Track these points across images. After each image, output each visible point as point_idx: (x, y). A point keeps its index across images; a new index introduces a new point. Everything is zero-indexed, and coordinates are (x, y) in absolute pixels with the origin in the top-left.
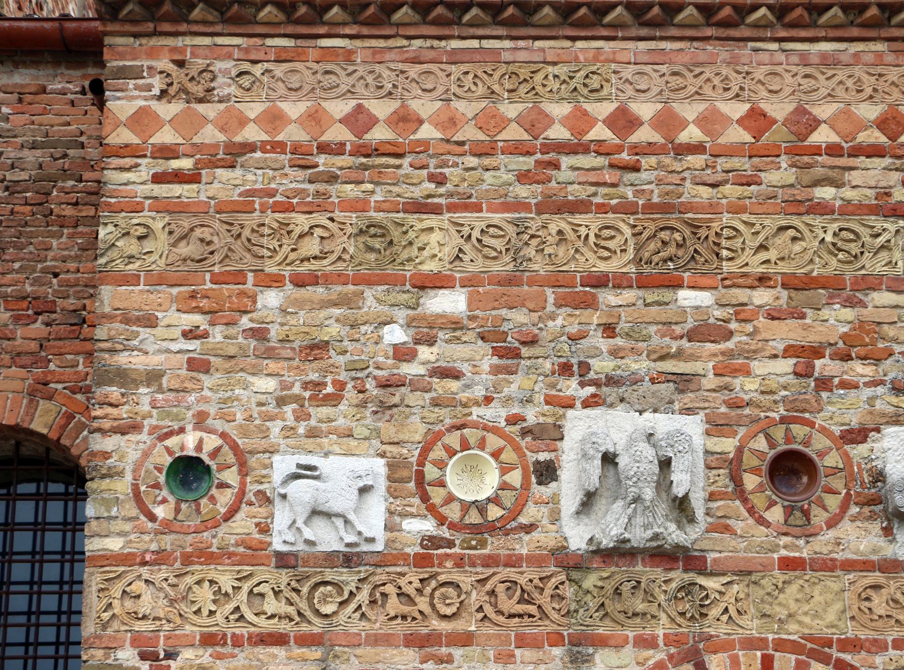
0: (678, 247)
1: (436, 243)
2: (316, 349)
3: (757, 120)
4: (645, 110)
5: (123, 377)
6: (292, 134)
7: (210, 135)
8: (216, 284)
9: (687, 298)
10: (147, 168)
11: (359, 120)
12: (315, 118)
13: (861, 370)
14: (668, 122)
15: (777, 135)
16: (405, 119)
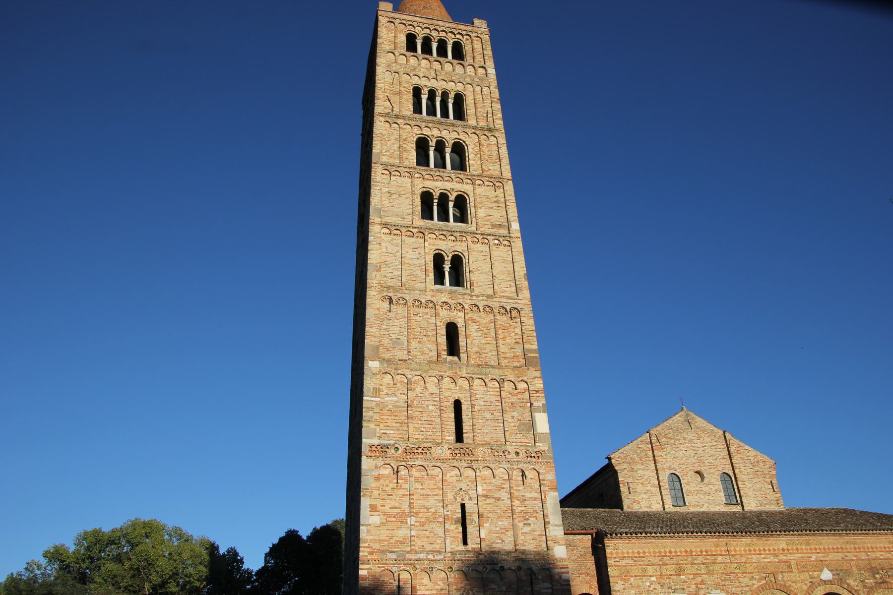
0: (680, 571)
1: (650, 570)
2: (639, 587)
3: (686, 551)
4: (673, 550)
5: (615, 591)
6: (631, 555)
7: (620, 555)
8: (625, 577)
9: (682, 577)
10: (613, 560)
11: (639, 553)
12: (633, 552)
13: (703, 586)
14: (676, 552)
15: (689, 554)
16: (644, 552)
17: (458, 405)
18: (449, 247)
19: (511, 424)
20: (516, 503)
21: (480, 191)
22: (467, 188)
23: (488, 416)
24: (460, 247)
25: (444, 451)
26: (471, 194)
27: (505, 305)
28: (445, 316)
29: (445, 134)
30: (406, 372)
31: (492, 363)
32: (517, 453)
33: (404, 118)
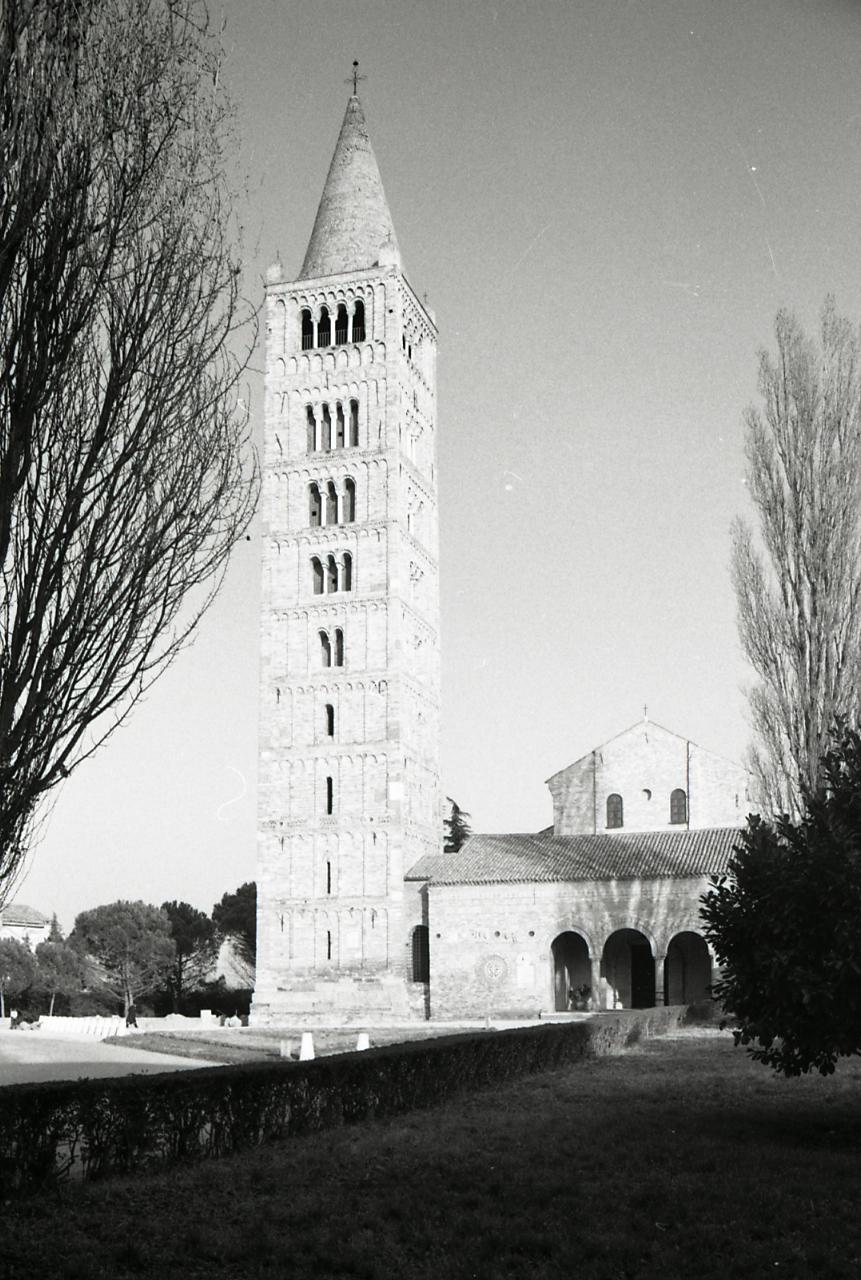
17: (330, 780)
18: (330, 626)
19: (370, 796)
20: (367, 859)
21: (364, 543)
22: (350, 545)
23: (352, 789)
24: (339, 622)
25: (315, 824)
26: (354, 551)
27: (373, 679)
28: (325, 698)
29: (333, 472)
30: (290, 758)
31: (360, 740)
32: (372, 819)
33: (292, 464)
